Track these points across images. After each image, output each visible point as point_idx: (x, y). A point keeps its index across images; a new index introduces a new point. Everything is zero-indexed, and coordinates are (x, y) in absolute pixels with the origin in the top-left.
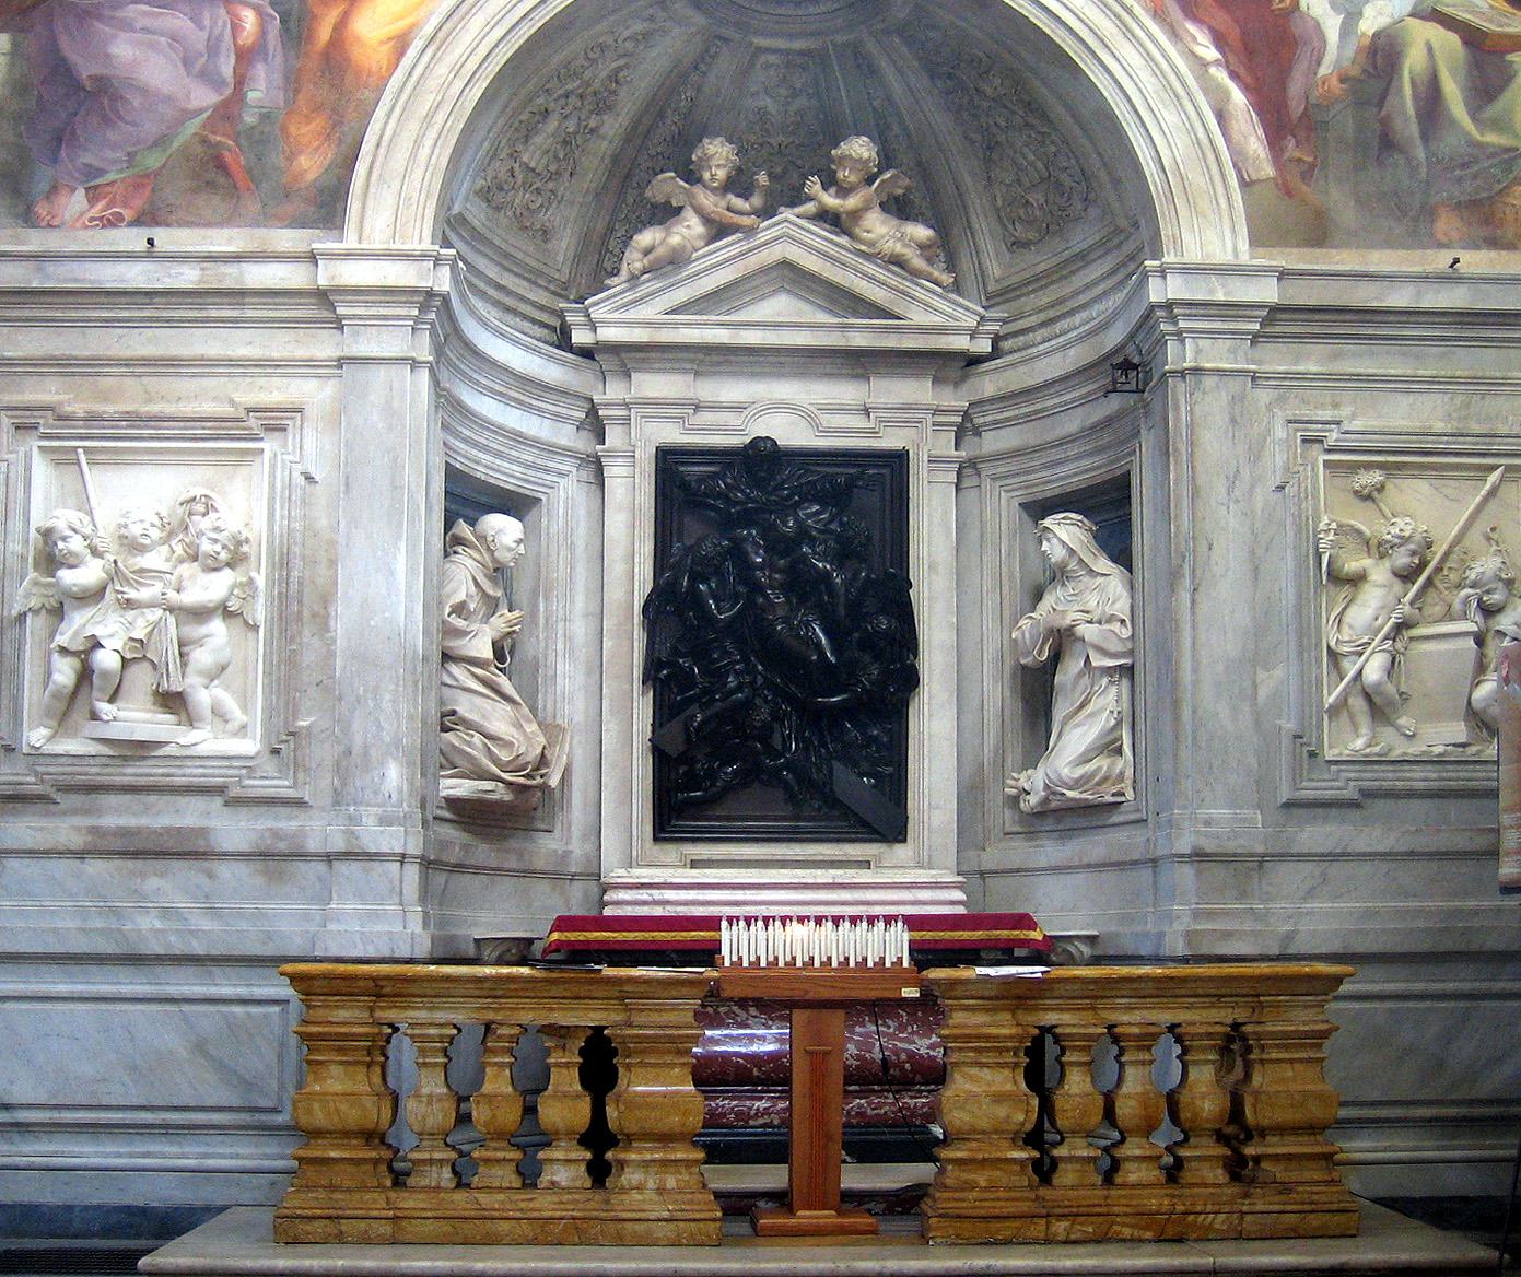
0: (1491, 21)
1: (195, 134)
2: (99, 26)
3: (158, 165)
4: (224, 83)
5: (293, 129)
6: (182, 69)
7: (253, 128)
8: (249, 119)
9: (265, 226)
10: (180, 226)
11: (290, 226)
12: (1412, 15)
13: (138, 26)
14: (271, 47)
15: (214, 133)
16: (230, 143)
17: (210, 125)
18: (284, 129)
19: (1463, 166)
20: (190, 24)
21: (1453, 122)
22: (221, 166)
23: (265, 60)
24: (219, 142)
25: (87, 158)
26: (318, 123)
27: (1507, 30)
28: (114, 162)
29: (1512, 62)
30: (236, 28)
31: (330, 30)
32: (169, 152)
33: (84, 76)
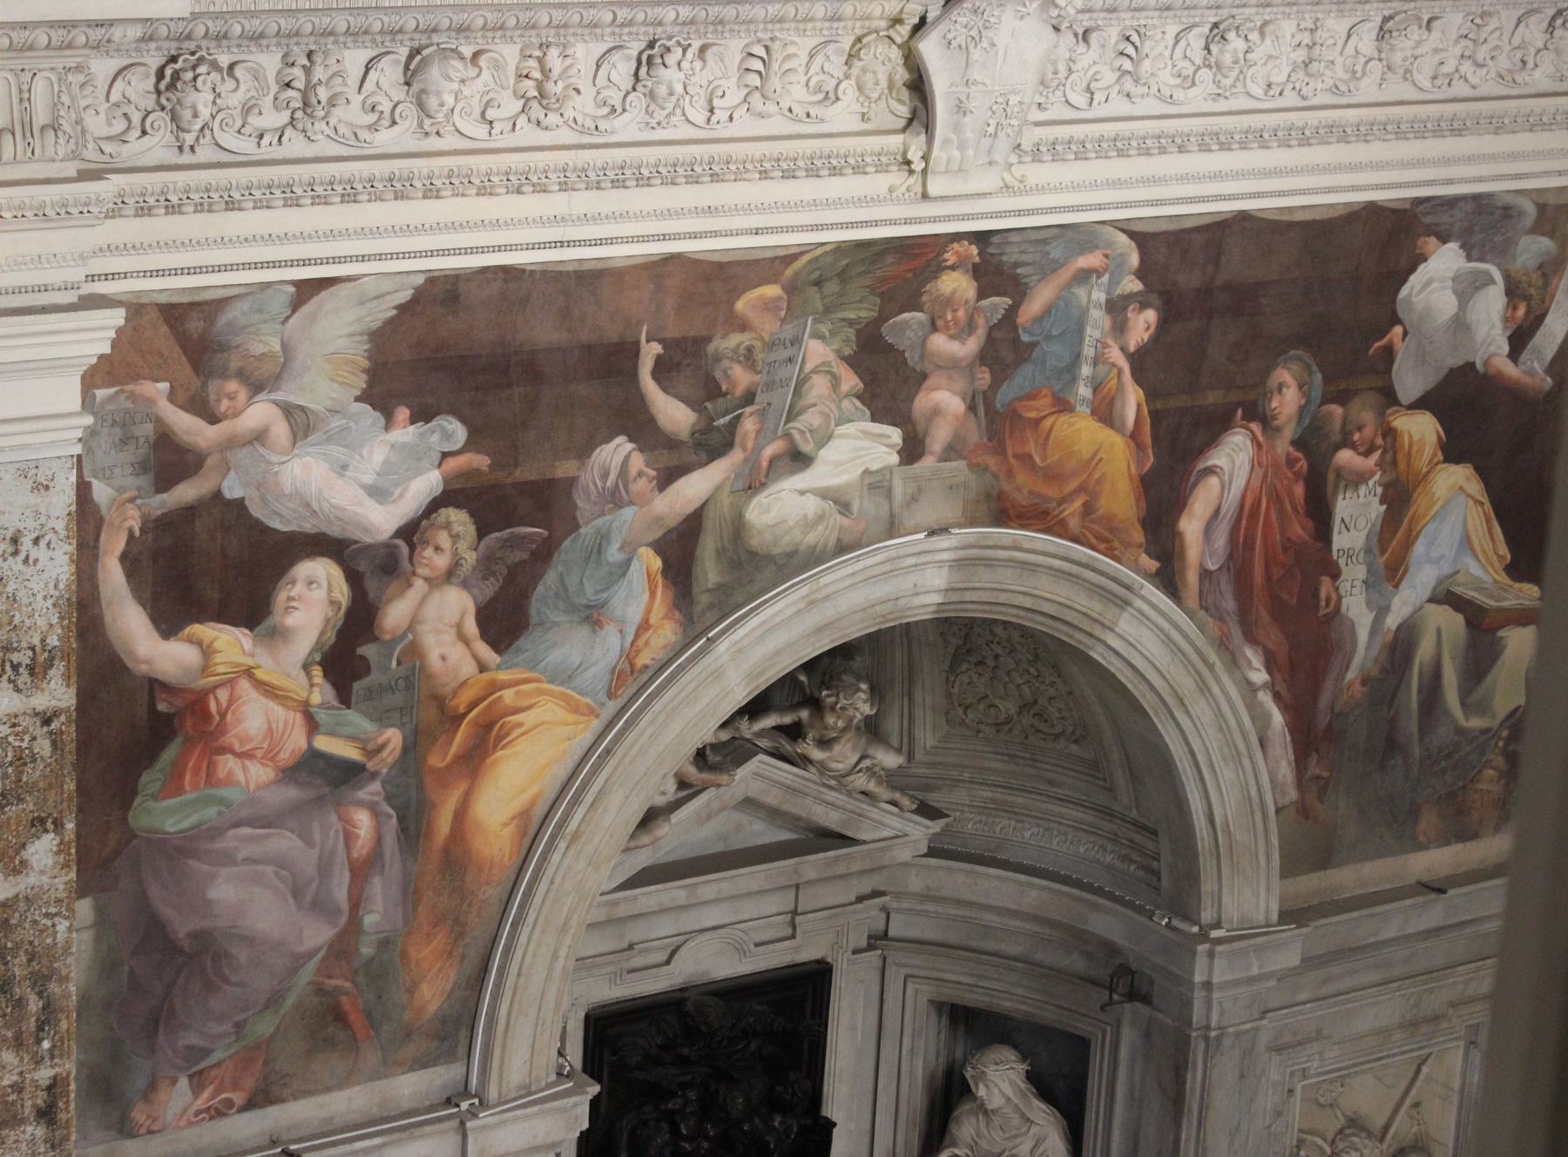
0: (1492, 597)
1: (309, 983)
2: (190, 862)
3: (271, 1030)
4: (338, 911)
5: (413, 954)
6: (291, 901)
7: (372, 960)
8: (367, 950)
9: (386, 1076)
10: (296, 1098)
11: (412, 1069)
12: (1431, 600)
13: (240, 856)
14: (387, 859)
15: (330, 977)
16: (348, 985)
17: (325, 970)
18: (404, 955)
19: (1448, 756)
20: (298, 842)
21: (1447, 712)
22: (340, 1017)
23: (382, 873)
24: (336, 986)
25: (193, 1039)
26: (440, 940)
27: (1505, 604)
28: (220, 1036)
29: (1502, 638)
30: (349, 838)
31: (450, 818)
32: (282, 1012)
33: (181, 935)
